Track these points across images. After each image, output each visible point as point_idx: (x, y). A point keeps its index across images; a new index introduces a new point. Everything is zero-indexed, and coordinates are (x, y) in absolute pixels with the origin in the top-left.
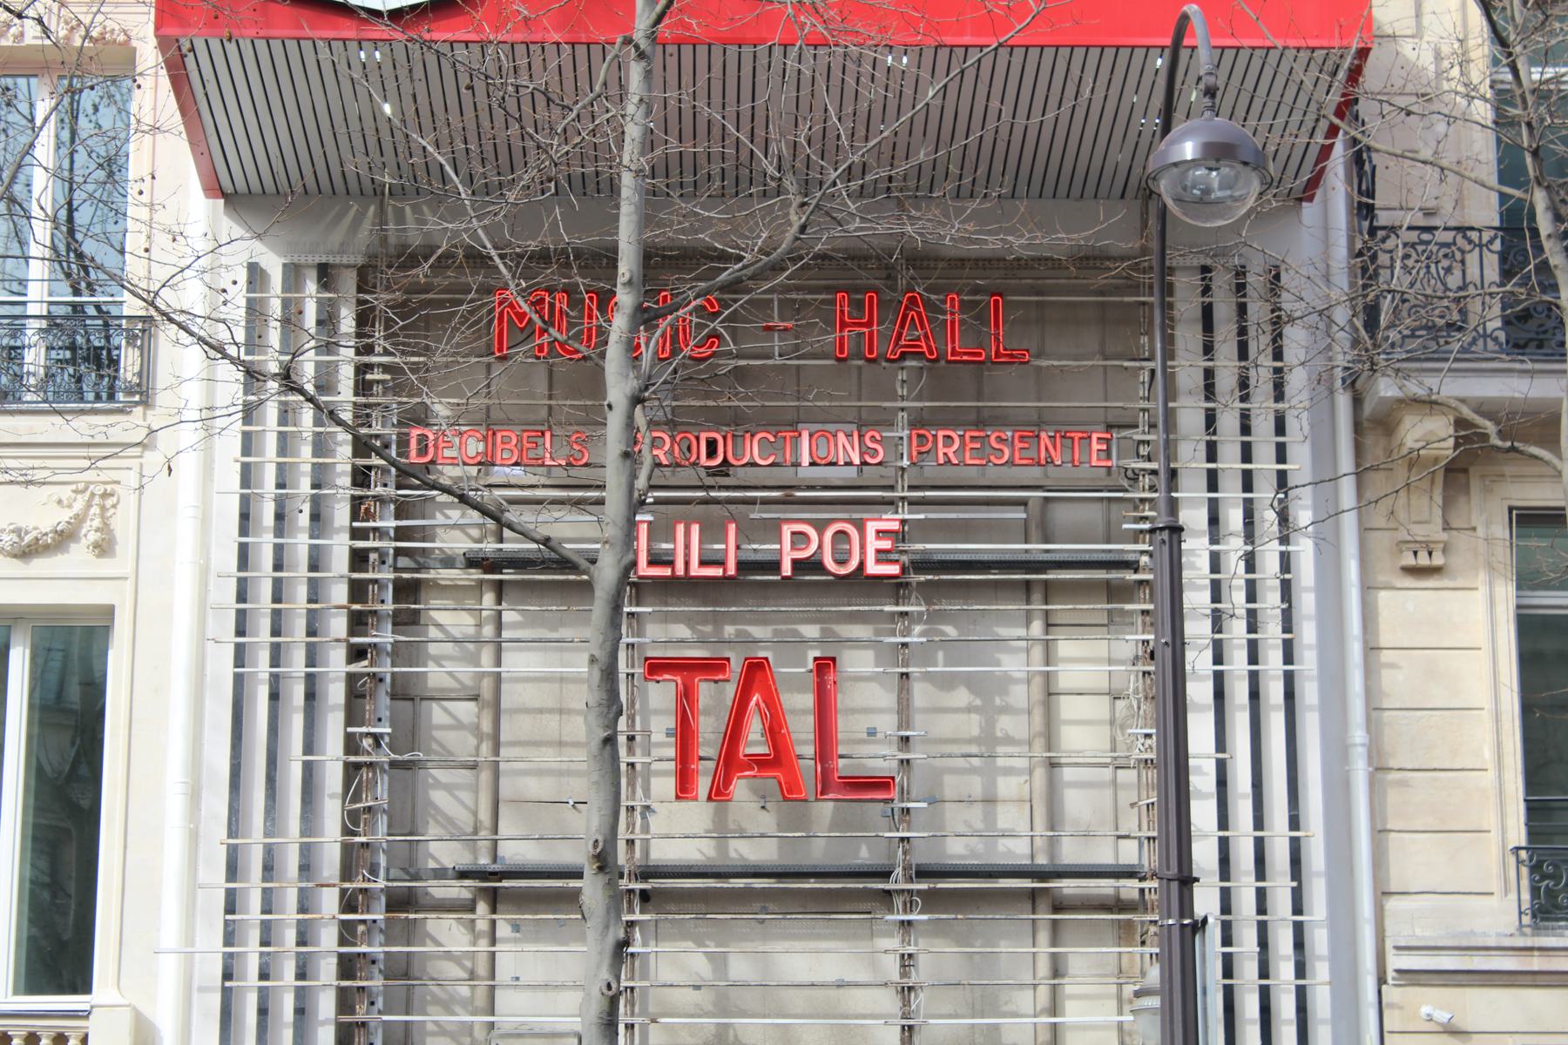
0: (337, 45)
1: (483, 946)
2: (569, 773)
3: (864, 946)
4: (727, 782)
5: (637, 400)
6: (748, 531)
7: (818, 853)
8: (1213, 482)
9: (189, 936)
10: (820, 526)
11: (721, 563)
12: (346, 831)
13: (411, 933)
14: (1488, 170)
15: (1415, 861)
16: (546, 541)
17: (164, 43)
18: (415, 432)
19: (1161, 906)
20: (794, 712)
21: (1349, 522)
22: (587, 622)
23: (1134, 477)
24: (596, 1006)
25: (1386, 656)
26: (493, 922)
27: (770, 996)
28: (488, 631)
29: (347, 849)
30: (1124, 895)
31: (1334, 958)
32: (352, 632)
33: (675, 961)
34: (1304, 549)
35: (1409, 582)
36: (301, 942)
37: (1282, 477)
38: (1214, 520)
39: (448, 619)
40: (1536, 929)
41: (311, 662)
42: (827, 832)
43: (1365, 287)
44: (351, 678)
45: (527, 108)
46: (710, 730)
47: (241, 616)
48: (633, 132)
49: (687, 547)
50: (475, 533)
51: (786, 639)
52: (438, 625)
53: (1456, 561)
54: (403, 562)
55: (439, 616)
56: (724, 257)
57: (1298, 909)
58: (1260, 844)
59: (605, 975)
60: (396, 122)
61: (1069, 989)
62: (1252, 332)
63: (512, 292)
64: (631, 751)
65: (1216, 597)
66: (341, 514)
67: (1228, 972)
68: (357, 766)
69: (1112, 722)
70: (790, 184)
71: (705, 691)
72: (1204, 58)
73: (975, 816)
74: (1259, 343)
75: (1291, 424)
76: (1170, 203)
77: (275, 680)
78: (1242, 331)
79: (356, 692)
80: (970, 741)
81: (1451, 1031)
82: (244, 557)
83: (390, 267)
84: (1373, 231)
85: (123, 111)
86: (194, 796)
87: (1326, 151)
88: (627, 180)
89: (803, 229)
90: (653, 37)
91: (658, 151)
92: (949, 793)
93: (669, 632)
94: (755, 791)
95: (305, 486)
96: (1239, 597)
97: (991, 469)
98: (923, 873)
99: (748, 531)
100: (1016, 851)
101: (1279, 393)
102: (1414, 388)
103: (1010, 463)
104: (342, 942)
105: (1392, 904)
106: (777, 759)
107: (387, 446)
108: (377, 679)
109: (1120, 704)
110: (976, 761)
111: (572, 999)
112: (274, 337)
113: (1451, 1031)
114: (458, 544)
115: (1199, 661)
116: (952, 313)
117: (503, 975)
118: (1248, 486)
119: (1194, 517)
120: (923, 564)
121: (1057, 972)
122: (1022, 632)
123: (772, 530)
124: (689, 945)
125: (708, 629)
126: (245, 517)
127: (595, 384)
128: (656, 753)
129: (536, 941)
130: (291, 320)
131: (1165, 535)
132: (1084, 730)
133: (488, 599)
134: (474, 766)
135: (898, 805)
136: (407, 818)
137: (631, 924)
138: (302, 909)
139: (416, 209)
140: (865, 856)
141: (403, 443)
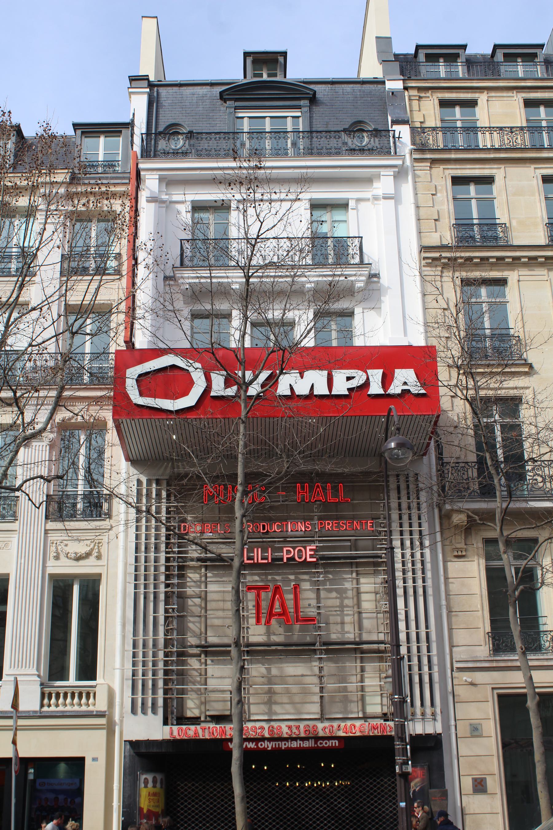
0: (161, 420)
1: (203, 667)
2: (226, 618)
3: (308, 665)
4: (270, 620)
5: (243, 516)
6: (274, 550)
7: (295, 638)
8: (401, 533)
9: (123, 665)
10: (294, 548)
11: (267, 559)
12: (165, 635)
13: (184, 663)
15: (460, 637)
16: (219, 555)
18: (183, 525)
19: (391, 651)
20: (288, 600)
21: (439, 545)
22: (231, 576)
23: (380, 533)
24: (235, 684)
25: (450, 580)
26: (206, 660)
27: (283, 679)
28: (203, 579)
29: (166, 640)
30: (380, 648)
31: (439, 665)
32: (166, 580)
33: (257, 670)
34: (427, 552)
35: (456, 560)
36: (153, 666)
37: (420, 532)
38: (402, 544)
39: (193, 576)
40: (494, 655)
41: (155, 588)
42: (297, 634)
43: (442, 480)
44: (166, 593)
45: (212, 437)
46: (264, 605)
47: (136, 576)
49: (258, 554)
50: (199, 552)
51: (286, 580)
52: (190, 577)
53: (468, 553)
54: (180, 560)
55: (189, 575)
56: (266, 476)
57: (429, 651)
58: (417, 634)
59: (238, 675)
60: (177, 441)
61: (366, 675)
62: (411, 493)
63: (209, 487)
64: (243, 612)
65: (403, 565)
66: (163, 547)
67: (410, 669)
68: (168, 617)
69: (376, 601)
70: (284, 456)
71: (263, 594)
72: (396, 419)
73: (339, 627)
74: (413, 496)
75: (422, 517)
76: (388, 459)
77: (145, 594)
78: (408, 493)
79: (168, 596)
80: (336, 607)
81: (472, 684)
82: (137, 559)
83: (176, 479)
84: (443, 464)
86: (124, 625)
88: (240, 456)
89: (288, 468)
91: (248, 448)
92: (331, 621)
93: (253, 579)
94: (277, 622)
95: (153, 540)
96: (410, 565)
97: (340, 531)
98: (325, 644)
99: (274, 550)
100: (350, 637)
101: (419, 509)
102: (455, 507)
103: (346, 529)
104: (165, 666)
105: (454, 649)
106: (284, 613)
107: (175, 528)
108: (173, 592)
109: (378, 595)
110: (338, 612)
111: (228, 681)
112: (144, 500)
113: (472, 684)
114: (195, 555)
115: (399, 583)
116: (329, 491)
117: (209, 674)
118: (411, 534)
119: (397, 543)
120: (323, 558)
121: (363, 670)
122: (350, 576)
123: (281, 550)
124: (260, 665)
125: (264, 577)
126: (137, 548)
127: (231, 510)
128: (250, 612)
129: (218, 664)
130: (149, 495)
131: (389, 550)
132: (368, 603)
133: (203, 570)
134: (200, 616)
135: (317, 625)
136: (182, 630)
137: (244, 660)
138: (153, 657)
139: (183, 465)
140: (308, 639)
141: (179, 529)
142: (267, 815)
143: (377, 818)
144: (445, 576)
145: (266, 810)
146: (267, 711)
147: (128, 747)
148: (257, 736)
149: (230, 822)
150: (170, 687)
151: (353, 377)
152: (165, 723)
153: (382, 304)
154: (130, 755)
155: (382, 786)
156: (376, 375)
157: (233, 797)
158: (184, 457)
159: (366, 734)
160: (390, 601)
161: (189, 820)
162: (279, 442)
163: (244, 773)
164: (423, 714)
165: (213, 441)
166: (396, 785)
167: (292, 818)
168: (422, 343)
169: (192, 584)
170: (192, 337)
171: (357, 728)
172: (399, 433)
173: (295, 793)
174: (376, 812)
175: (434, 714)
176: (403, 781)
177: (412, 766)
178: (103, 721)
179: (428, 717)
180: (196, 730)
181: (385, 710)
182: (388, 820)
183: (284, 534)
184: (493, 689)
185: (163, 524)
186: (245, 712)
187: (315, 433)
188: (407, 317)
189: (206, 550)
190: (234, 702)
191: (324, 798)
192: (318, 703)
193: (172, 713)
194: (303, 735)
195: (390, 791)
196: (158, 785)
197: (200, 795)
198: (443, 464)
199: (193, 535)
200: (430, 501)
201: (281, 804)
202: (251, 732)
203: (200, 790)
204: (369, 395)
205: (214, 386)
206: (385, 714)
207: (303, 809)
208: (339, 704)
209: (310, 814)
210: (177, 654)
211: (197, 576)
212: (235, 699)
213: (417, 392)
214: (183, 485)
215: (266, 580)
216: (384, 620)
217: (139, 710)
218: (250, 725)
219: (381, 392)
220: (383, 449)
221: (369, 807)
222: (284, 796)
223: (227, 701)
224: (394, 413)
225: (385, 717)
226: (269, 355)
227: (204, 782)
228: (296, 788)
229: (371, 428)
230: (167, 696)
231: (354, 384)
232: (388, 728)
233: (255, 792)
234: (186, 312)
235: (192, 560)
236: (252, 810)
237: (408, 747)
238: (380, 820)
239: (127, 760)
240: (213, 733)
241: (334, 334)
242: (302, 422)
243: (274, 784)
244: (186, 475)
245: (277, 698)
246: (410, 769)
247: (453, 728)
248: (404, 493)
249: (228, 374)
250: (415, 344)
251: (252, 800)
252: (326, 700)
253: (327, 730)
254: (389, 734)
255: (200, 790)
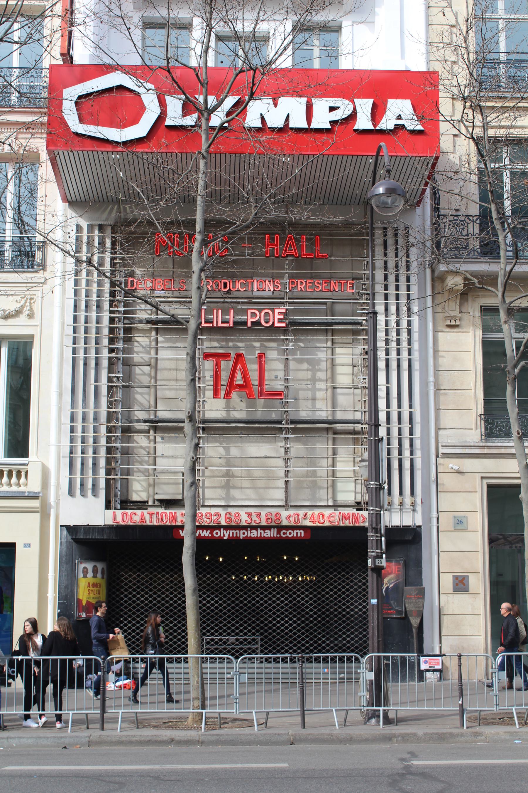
0: (105, 153)
1: (152, 444)
2: (179, 389)
3: (273, 445)
4: (230, 393)
5: (202, 270)
7: (259, 415)
8: (386, 297)
9: (59, 440)
10: (260, 311)
11: (228, 322)
12: (108, 407)
13: (129, 440)
14: (476, 198)
15: (449, 419)
16: (173, 316)
17: (49, 152)
18: (130, 279)
19: (369, 434)
20: (251, 370)
21: (430, 311)
22: (186, 341)
23: (361, 295)
24: (189, 464)
25: (441, 353)
26: (155, 437)
27: (244, 460)
28: (153, 344)
29: (109, 413)
30: (356, 429)
32: (110, 344)
33: (213, 450)
34: (415, 319)
35: (448, 330)
37: (408, 296)
38: (386, 310)
39: (141, 340)
40: (486, 440)
41: (97, 353)
42: (261, 410)
43: (436, 235)
44: (110, 359)
45: (166, 174)
46: (224, 376)
48: (201, 183)
49: (217, 317)
50: (149, 312)
51: (249, 347)
52: (137, 342)
53: (463, 323)
55: (138, 339)
57: (411, 434)
58: (399, 413)
59: (192, 454)
60: (125, 178)
61: (338, 459)
62: (400, 249)
63: (162, 235)
64: (199, 383)
65: (387, 335)
66: (106, 306)
67: (389, 453)
68: (112, 387)
69: (353, 374)
70: (252, 200)
71: (223, 363)
72: (386, 159)
73: (309, 404)
74: (402, 253)
75: (412, 279)
77: (85, 359)
78: (397, 249)
79: (111, 363)
80: (307, 380)
81: (459, 472)
82: (75, 318)
83: (122, 226)
84: (439, 216)
85: (36, 174)
86: (60, 396)
87: (424, 191)
88: (199, 198)
89: (256, 214)
90: (207, 151)
92: (301, 397)
94: (239, 395)
95: (94, 297)
96: (394, 334)
97: (315, 293)
100: (322, 415)
101: (408, 268)
102: (451, 268)
103: (321, 291)
105: (441, 432)
106: (246, 385)
107: (121, 284)
109: (356, 368)
111: (181, 461)
112: (85, 248)
113: (459, 472)
114: (144, 316)
115: (381, 355)
116: (303, 243)
117: (159, 452)
118: (397, 298)
119: (380, 309)
120: (293, 323)
121: (335, 453)
122: (325, 345)
123: (245, 312)
124: (218, 444)
125: (224, 343)
126: (75, 306)
127: (188, 264)
128: (207, 383)
129: (169, 443)
130: (90, 243)
131: (372, 315)
132: (345, 377)
133: (153, 333)
134: (149, 387)
135: (284, 400)
136: (128, 403)
137: (199, 438)
138: (95, 432)
139: (130, 208)
140: (274, 417)
141: (126, 283)
142: (221, 611)
143: (344, 616)
144: (434, 349)
145: (221, 605)
146: (224, 496)
147: (65, 532)
148: (212, 524)
149: (179, 616)
150: (113, 466)
151: (338, 107)
152: (108, 506)
153: (376, 17)
154: (67, 542)
155: (352, 581)
156: (365, 106)
157: (184, 590)
158: (133, 199)
159: (336, 524)
160: (369, 375)
161: (134, 613)
162: (246, 183)
163: (197, 564)
164: (401, 504)
165: (167, 179)
166: (367, 581)
167: (249, 614)
168: (423, 68)
169: (141, 349)
170: (144, 50)
171: (325, 518)
172: (389, 177)
173: (254, 588)
174: (344, 610)
175: (413, 504)
176: (375, 575)
177: (387, 561)
178: (36, 503)
179: (407, 507)
180: (143, 515)
181: (359, 499)
182: (356, 619)
183: (249, 294)
184: (482, 478)
185: (107, 277)
186: (199, 497)
187: (289, 173)
188: (406, 33)
189: (157, 309)
190: (187, 485)
191: (286, 593)
192: (282, 488)
193: (116, 496)
194: (264, 523)
195: (360, 587)
196: (99, 575)
197: (147, 587)
198: (439, 216)
199: (142, 292)
200: (422, 259)
201: (237, 599)
202: (205, 519)
203: (147, 582)
204: (356, 130)
205: (170, 112)
206: (358, 503)
207: (262, 605)
208: (306, 490)
209: (270, 611)
210: (121, 428)
211: (147, 340)
212: (188, 481)
213: (411, 128)
214: (131, 233)
215: (226, 347)
216: (361, 397)
217: (78, 491)
218: (204, 511)
219: (370, 126)
220: (369, 195)
221: (336, 604)
222: (241, 590)
223: (179, 484)
224: (385, 151)
225: (358, 506)
226: (237, 75)
227: (151, 573)
228: (254, 581)
229: (356, 170)
230: (109, 477)
231: (337, 115)
232: (361, 519)
233: (209, 585)
234: (136, 18)
235: (141, 321)
236: (204, 605)
237: (383, 539)
238: (348, 619)
239: (64, 547)
240: (162, 519)
241: (316, 52)
242: (274, 160)
243: (230, 576)
244: (135, 220)
245: (235, 482)
246: (383, 563)
247: (435, 521)
248: (391, 249)
249: (187, 98)
250: (413, 69)
251: (204, 593)
252: (292, 485)
253: (291, 519)
254: (362, 525)
255: (147, 582)
